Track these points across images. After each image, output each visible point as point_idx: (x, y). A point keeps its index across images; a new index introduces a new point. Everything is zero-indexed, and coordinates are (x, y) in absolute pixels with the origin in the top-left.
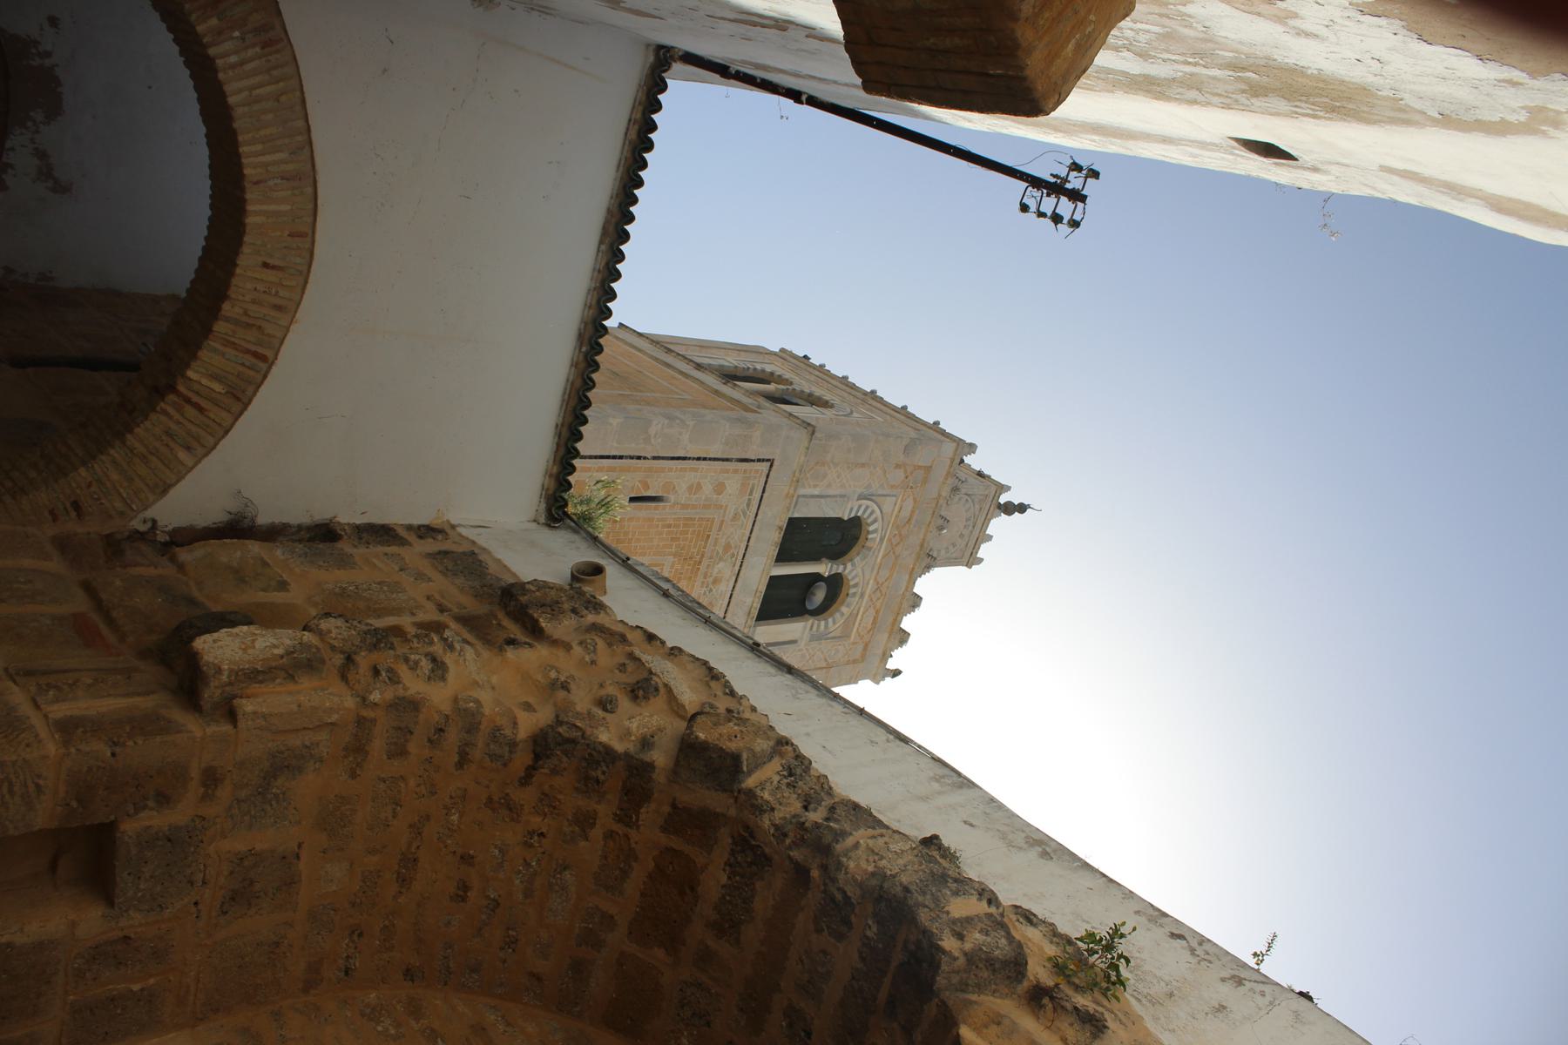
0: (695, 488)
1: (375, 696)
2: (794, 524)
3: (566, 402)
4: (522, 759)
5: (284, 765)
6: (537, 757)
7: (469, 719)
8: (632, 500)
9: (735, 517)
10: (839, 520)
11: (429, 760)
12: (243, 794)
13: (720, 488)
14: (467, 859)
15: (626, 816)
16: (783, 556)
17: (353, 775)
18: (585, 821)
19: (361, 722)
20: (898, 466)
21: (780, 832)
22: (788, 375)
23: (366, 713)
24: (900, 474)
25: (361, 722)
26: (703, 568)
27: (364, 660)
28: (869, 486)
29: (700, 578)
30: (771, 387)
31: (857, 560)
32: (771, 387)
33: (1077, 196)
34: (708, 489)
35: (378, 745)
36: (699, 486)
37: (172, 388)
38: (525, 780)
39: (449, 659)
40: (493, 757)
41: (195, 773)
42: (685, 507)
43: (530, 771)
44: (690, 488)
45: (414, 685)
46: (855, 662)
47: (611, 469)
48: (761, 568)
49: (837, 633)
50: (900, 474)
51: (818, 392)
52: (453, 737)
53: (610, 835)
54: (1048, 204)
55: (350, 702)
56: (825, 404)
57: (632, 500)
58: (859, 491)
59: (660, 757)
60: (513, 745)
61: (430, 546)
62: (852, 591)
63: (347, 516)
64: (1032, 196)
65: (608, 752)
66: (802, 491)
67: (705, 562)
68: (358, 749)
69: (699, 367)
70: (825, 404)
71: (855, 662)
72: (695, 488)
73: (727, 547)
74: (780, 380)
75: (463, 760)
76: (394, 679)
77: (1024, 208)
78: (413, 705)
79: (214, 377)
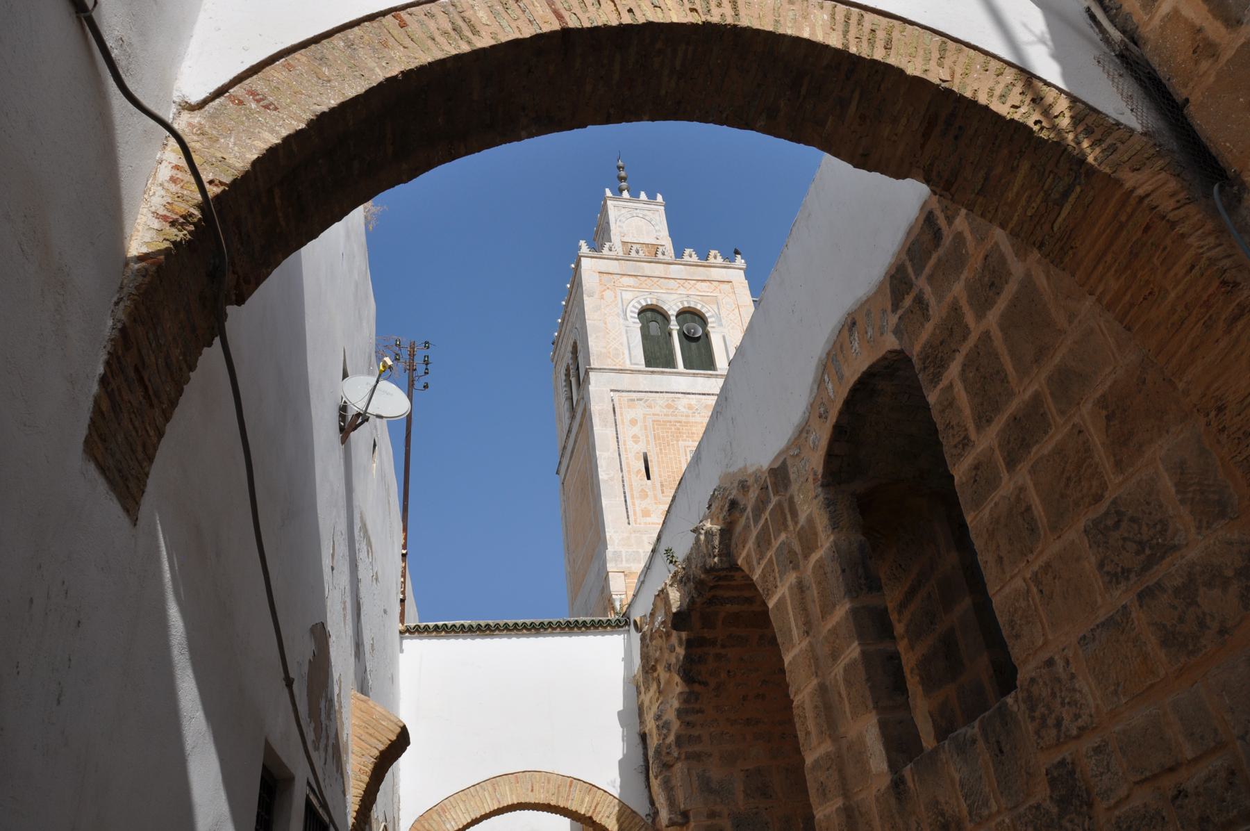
0: (636, 438)
1: (676, 755)
2: (648, 364)
3: (570, 634)
4: (697, 687)
5: (706, 786)
6: (694, 682)
7: (680, 713)
8: (649, 478)
9: (650, 407)
10: (641, 328)
11: (702, 725)
12: (719, 800)
13: (633, 422)
14: (745, 698)
15: (713, 643)
16: (670, 363)
17: (710, 755)
18: (718, 657)
19: (687, 758)
20: (602, 298)
21: (700, 594)
22: (565, 365)
23: (683, 756)
24: (608, 294)
25: (687, 758)
26: (684, 419)
27: (666, 759)
28: (618, 315)
29: (691, 419)
30: (573, 380)
31: (665, 308)
32: (573, 380)
33: (412, 346)
34: (636, 430)
35: (697, 748)
36: (635, 436)
37: (591, 818)
38: (705, 684)
39: (664, 719)
40: (697, 699)
41: (709, 823)
42: (648, 442)
43: (700, 683)
44: (636, 442)
45: (671, 738)
46: (733, 288)
47: (632, 497)
48: (681, 380)
49: (715, 307)
50: (608, 294)
51: (570, 348)
52: (691, 718)
53: (723, 646)
54: (421, 369)
55: (679, 765)
56: (575, 343)
57: (649, 478)
58: (622, 321)
59: (684, 635)
60: (691, 693)
61: (643, 689)
62: (686, 305)
63: (637, 728)
64: (419, 385)
65: (685, 657)
66: (628, 362)
67: (679, 418)
68: (697, 757)
69: (569, 431)
70: (575, 343)
71: (733, 288)
72: (636, 438)
73: (669, 406)
74: (568, 370)
75: (701, 711)
76: (669, 746)
77: (426, 387)
78: (678, 738)
79: (582, 802)
